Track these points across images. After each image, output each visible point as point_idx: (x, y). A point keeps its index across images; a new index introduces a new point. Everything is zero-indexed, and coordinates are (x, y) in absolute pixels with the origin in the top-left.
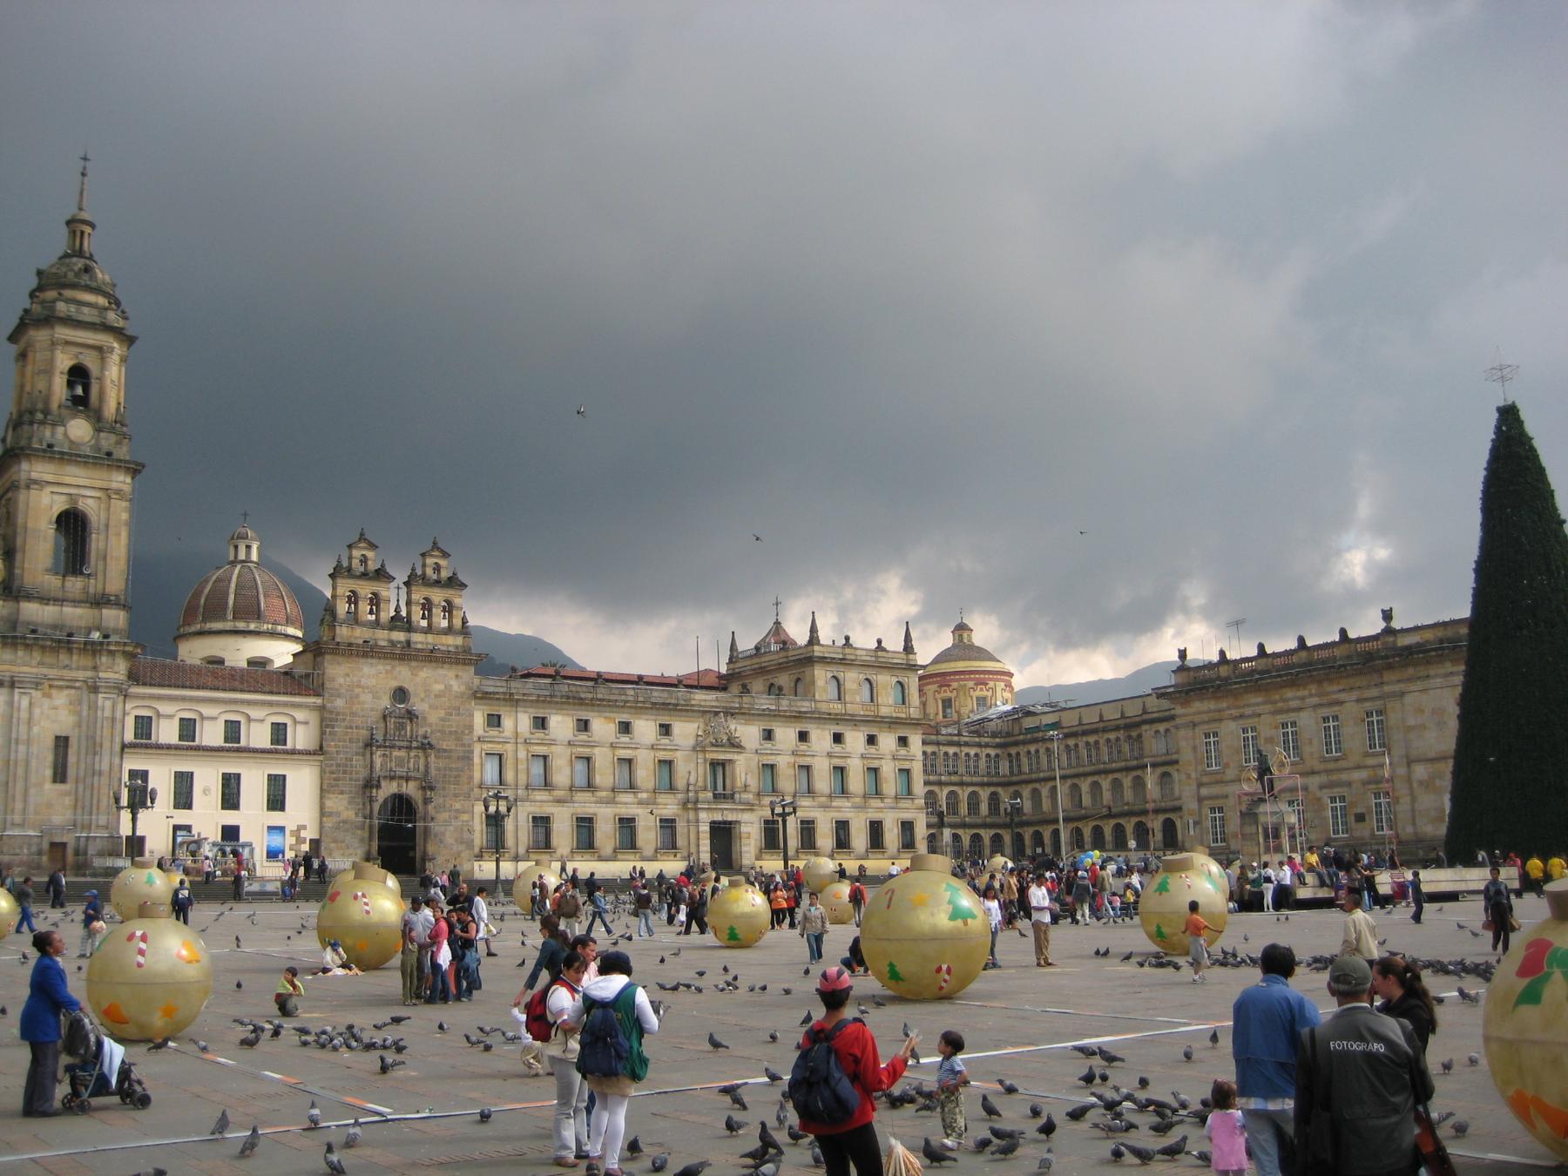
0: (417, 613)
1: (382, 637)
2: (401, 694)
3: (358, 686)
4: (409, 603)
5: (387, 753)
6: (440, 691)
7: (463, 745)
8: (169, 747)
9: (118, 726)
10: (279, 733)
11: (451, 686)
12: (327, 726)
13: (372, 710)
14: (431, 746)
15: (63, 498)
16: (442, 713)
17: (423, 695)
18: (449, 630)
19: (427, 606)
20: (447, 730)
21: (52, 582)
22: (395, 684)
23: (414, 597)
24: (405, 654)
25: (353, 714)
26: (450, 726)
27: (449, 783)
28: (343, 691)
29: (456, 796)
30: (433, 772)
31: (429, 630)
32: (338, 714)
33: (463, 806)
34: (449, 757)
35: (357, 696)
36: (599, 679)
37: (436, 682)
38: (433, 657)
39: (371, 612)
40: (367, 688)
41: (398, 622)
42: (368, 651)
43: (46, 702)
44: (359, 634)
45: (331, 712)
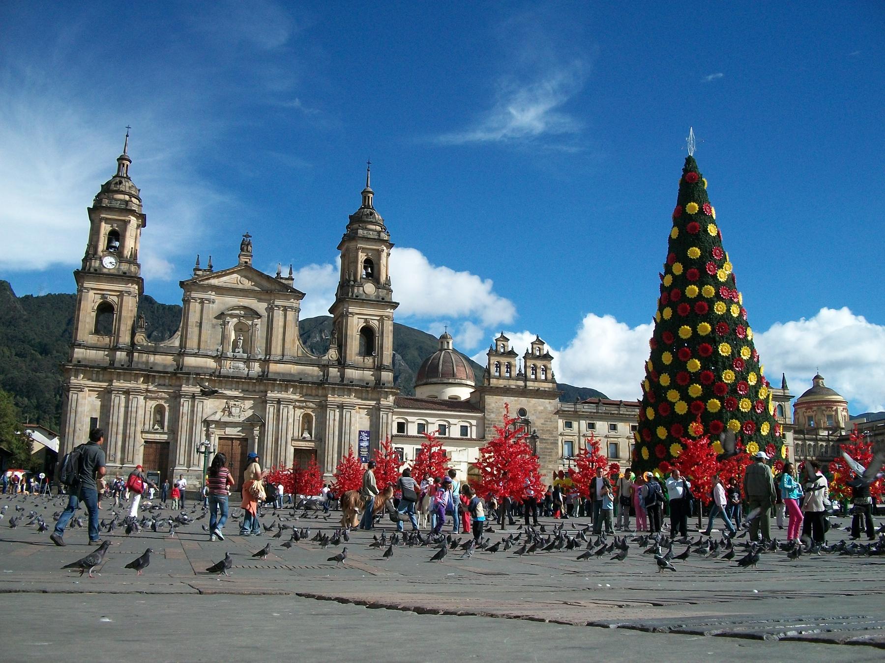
0: (529, 372)
1: (513, 384)
2: (522, 412)
4: (525, 367)
6: (542, 410)
7: (552, 437)
8: (414, 437)
9: (389, 427)
10: (464, 430)
14: (538, 437)
15: (363, 320)
16: (542, 421)
17: (533, 412)
18: (546, 380)
19: (535, 369)
20: (545, 429)
21: (360, 359)
22: (519, 407)
23: (528, 364)
24: (524, 392)
26: (548, 427)
27: (546, 455)
28: (495, 410)
29: (550, 462)
30: (538, 450)
31: (536, 380)
33: (553, 466)
34: (545, 443)
36: (619, 404)
37: (540, 406)
38: (538, 394)
39: (507, 372)
41: (523, 377)
42: (506, 391)
43: (358, 416)
44: (502, 383)
45: (489, 420)
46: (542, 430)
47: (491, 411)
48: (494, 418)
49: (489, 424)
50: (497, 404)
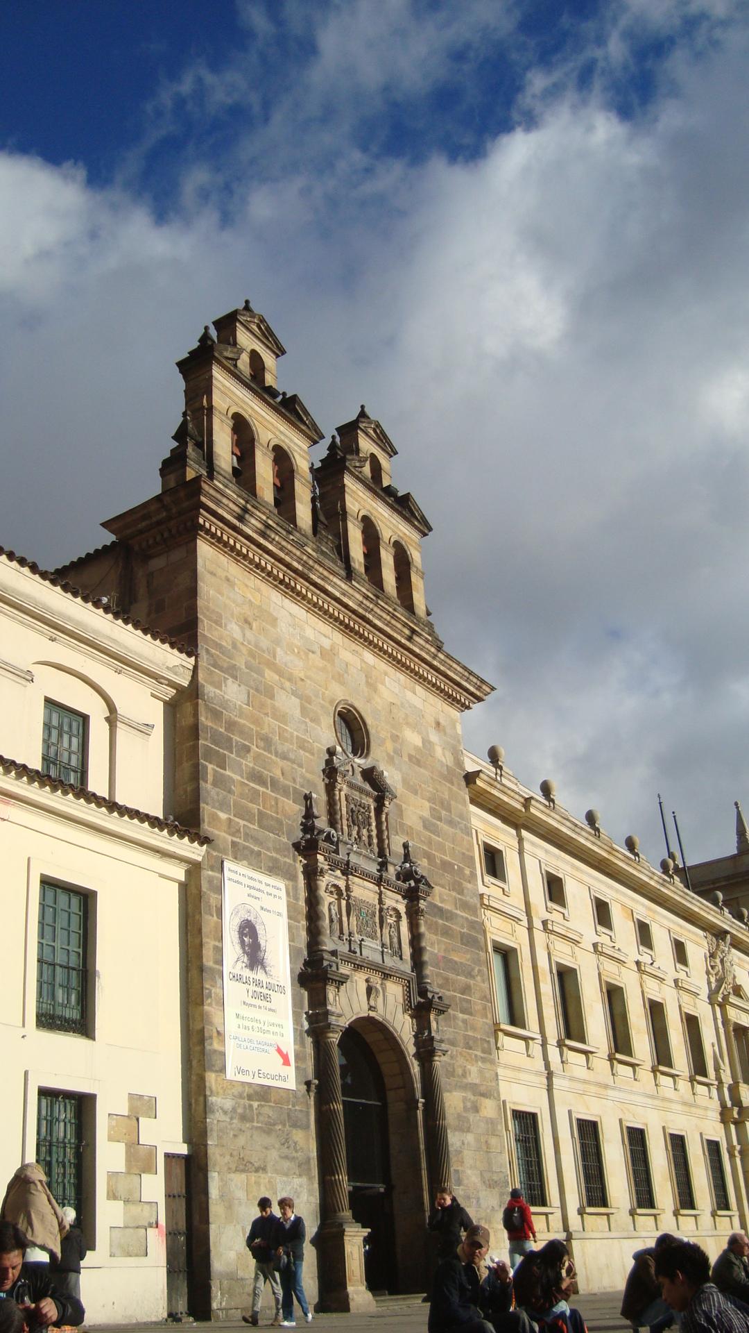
7: (465, 906)
11: (430, 742)
12: (210, 755)
22: (340, 693)
25: (267, 742)
28: (240, 662)
32: (231, 725)
45: (216, 715)
47: (224, 661)
48: (241, 714)
49: (216, 739)
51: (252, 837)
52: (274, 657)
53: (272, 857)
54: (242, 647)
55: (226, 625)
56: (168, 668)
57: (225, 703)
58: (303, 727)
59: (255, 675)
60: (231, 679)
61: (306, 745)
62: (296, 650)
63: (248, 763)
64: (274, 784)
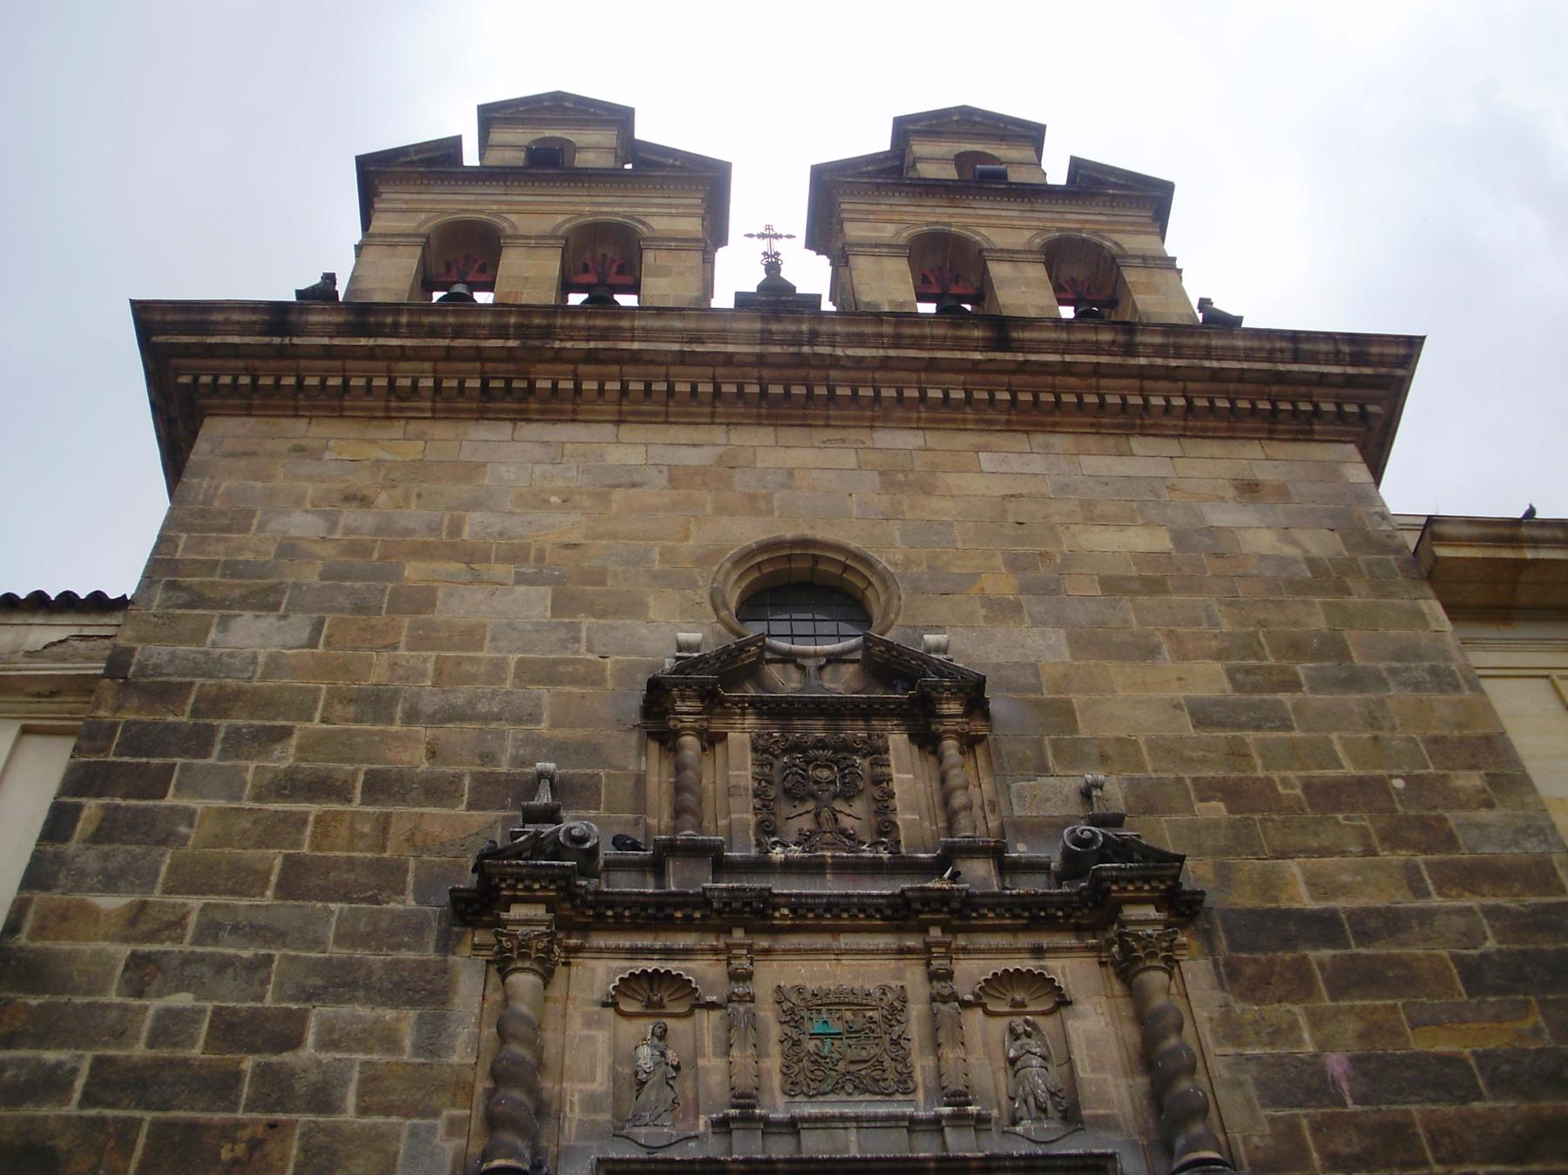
3: (424, 552)
5: (705, 971)
6: (1150, 558)
13: (547, 673)
20: (1289, 781)
25: (377, 704)
32: (219, 702)
35: (421, 600)
37: (1092, 516)
40: (516, 555)
46: (1231, 793)
48: (275, 665)
50: (351, 516)
51: (236, 929)
52: (456, 529)
53: (328, 960)
54: (316, 549)
55: (262, 526)
56: (30, 654)
57: (209, 667)
58: (562, 633)
59: (358, 585)
60: (248, 615)
61: (562, 669)
62: (554, 499)
63: (284, 758)
64: (378, 786)
